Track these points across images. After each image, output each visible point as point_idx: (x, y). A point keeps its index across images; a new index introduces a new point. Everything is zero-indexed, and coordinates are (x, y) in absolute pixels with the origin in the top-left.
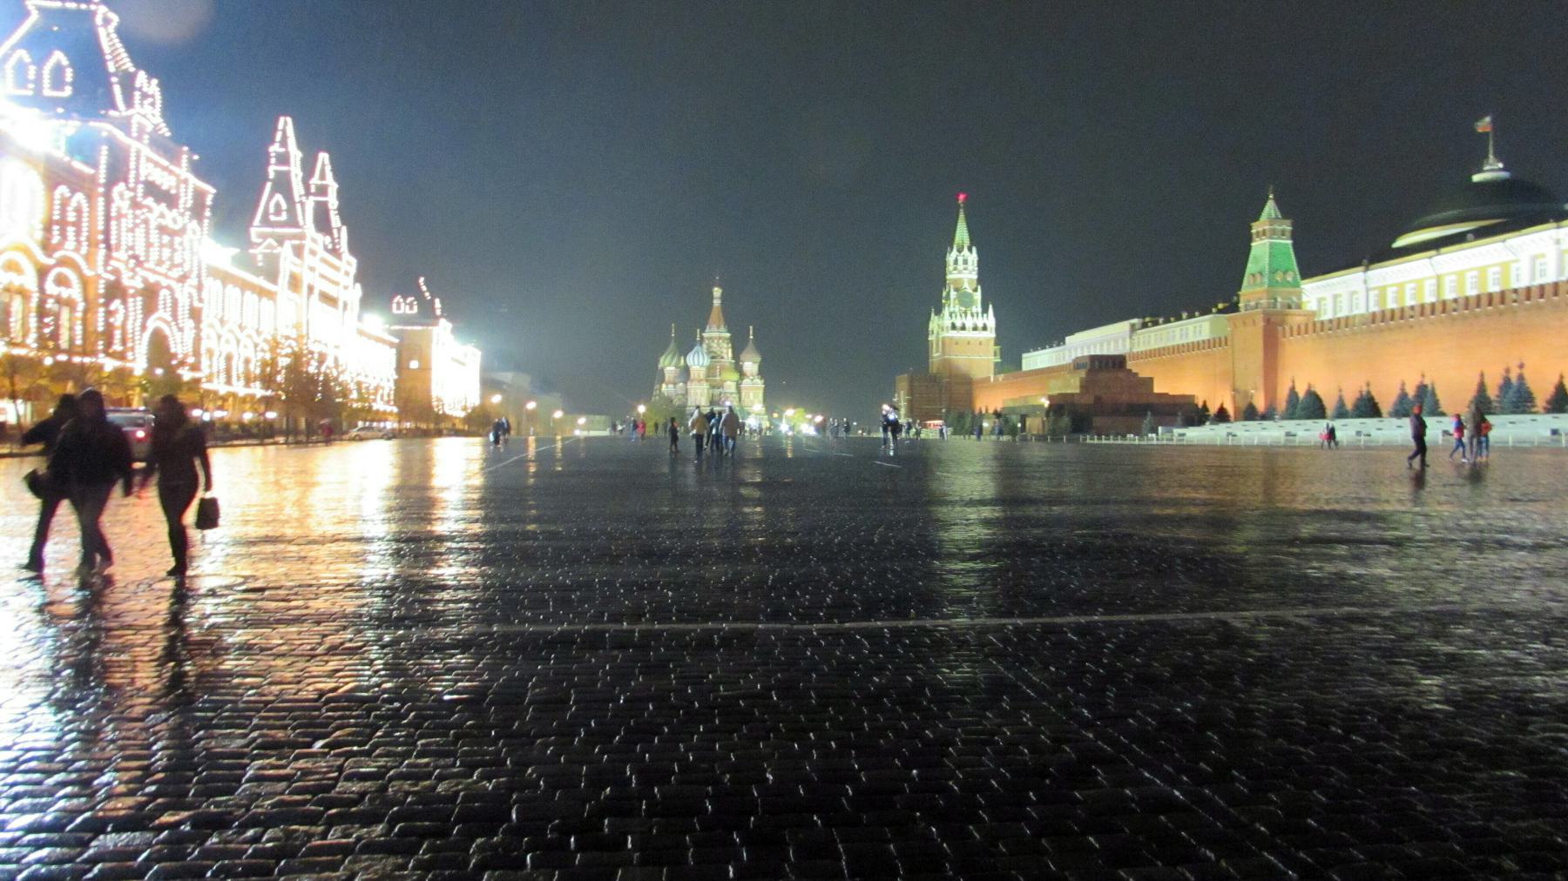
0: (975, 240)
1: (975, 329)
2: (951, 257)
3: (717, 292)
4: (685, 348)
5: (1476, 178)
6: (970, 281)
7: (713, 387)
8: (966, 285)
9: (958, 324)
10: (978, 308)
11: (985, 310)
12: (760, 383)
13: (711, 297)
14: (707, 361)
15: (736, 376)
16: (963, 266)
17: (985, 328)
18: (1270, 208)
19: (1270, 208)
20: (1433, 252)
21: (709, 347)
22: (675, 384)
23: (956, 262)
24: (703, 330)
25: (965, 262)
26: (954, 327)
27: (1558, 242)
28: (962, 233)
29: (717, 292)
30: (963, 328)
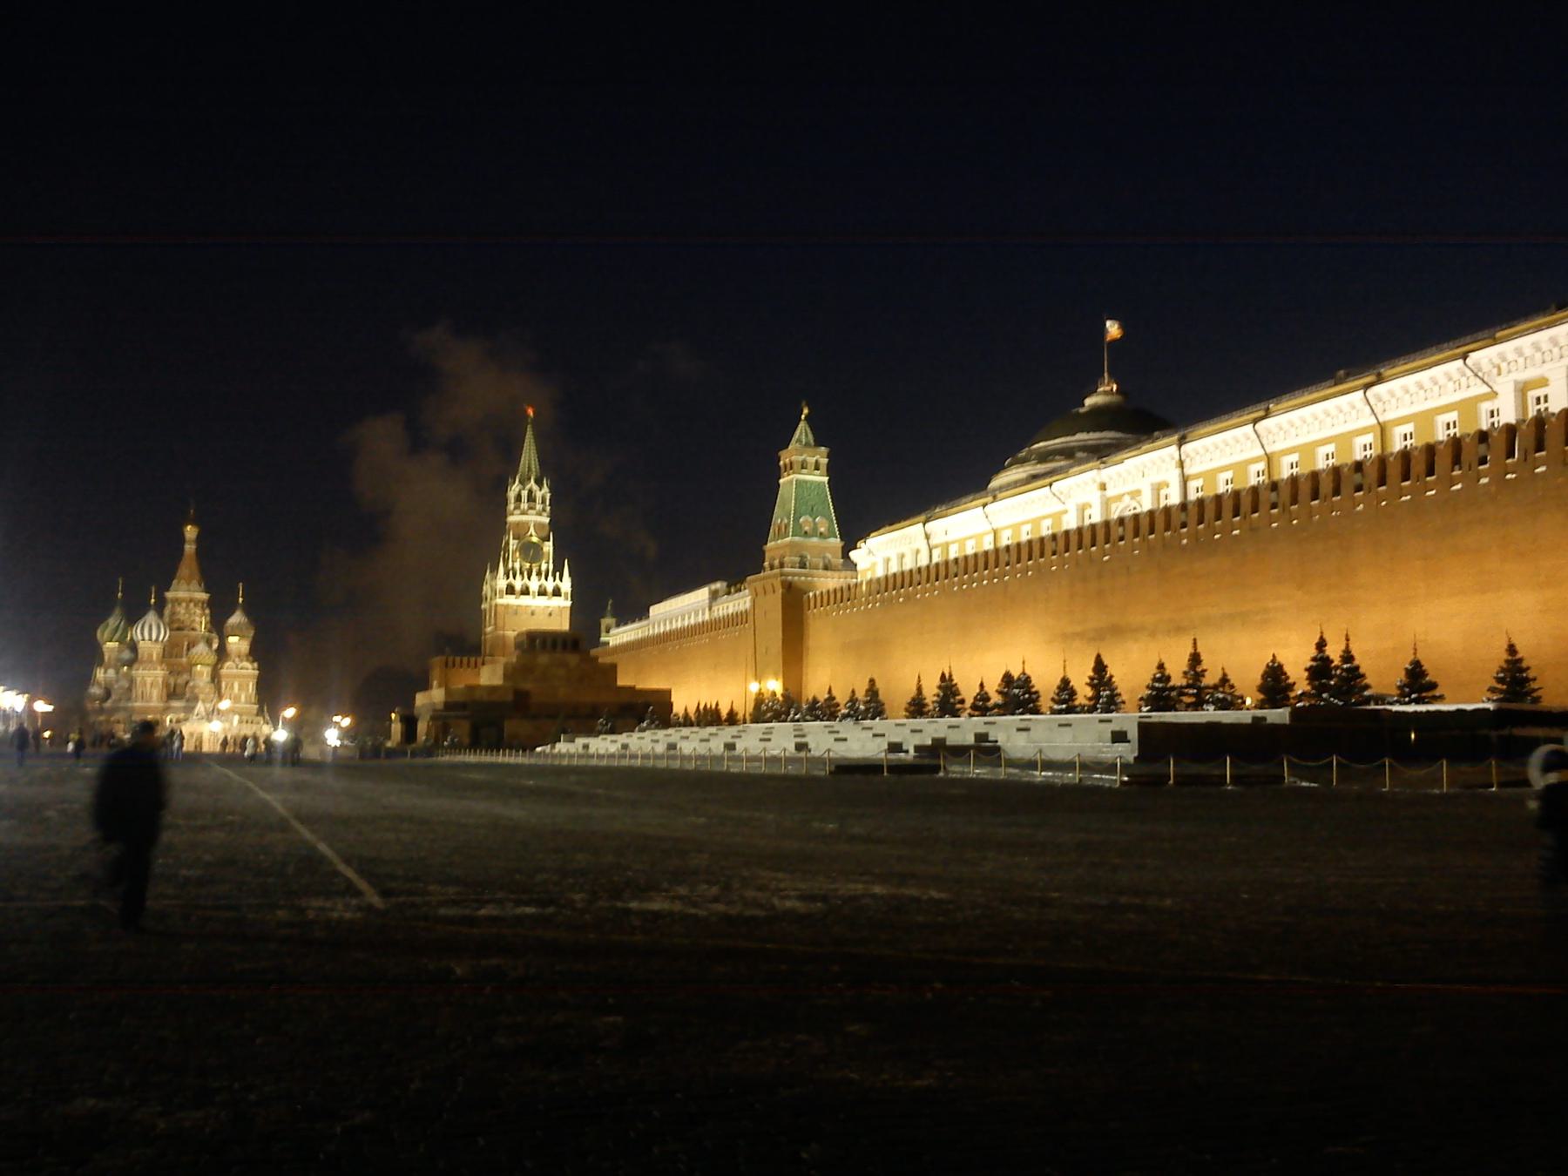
1: (542, 593)
2: (512, 494)
3: (190, 531)
6: (538, 526)
8: (532, 530)
9: (518, 584)
10: (547, 565)
11: (558, 568)
12: (250, 670)
13: (182, 540)
14: (164, 635)
16: (529, 509)
17: (557, 592)
18: (803, 431)
19: (803, 431)
21: (173, 613)
23: (518, 498)
25: (531, 498)
26: (510, 590)
27: (1103, 487)
28: (529, 456)
29: (190, 531)
30: (525, 591)
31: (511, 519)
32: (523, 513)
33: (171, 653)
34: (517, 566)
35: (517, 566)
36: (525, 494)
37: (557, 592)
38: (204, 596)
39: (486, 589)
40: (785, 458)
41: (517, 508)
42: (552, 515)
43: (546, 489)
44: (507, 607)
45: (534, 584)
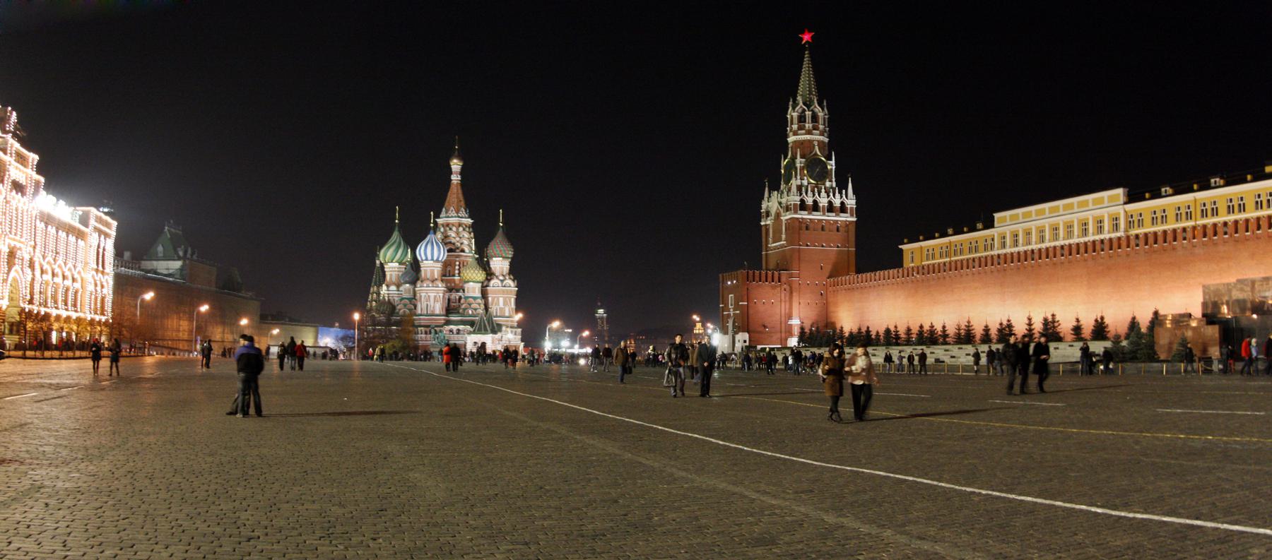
1: (831, 208)
3: (456, 165)
4: (413, 239)
6: (820, 143)
7: (450, 290)
9: (809, 201)
11: (842, 186)
12: (511, 284)
15: (480, 275)
17: (843, 209)
22: (398, 286)
23: (802, 119)
24: (437, 216)
26: (803, 206)
29: (456, 165)
30: (816, 207)
31: (791, 139)
32: (809, 132)
33: (448, 270)
34: (805, 182)
35: (805, 182)
36: (808, 113)
37: (843, 209)
38: (470, 221)
39: (771, 203)
41: (800, 128)
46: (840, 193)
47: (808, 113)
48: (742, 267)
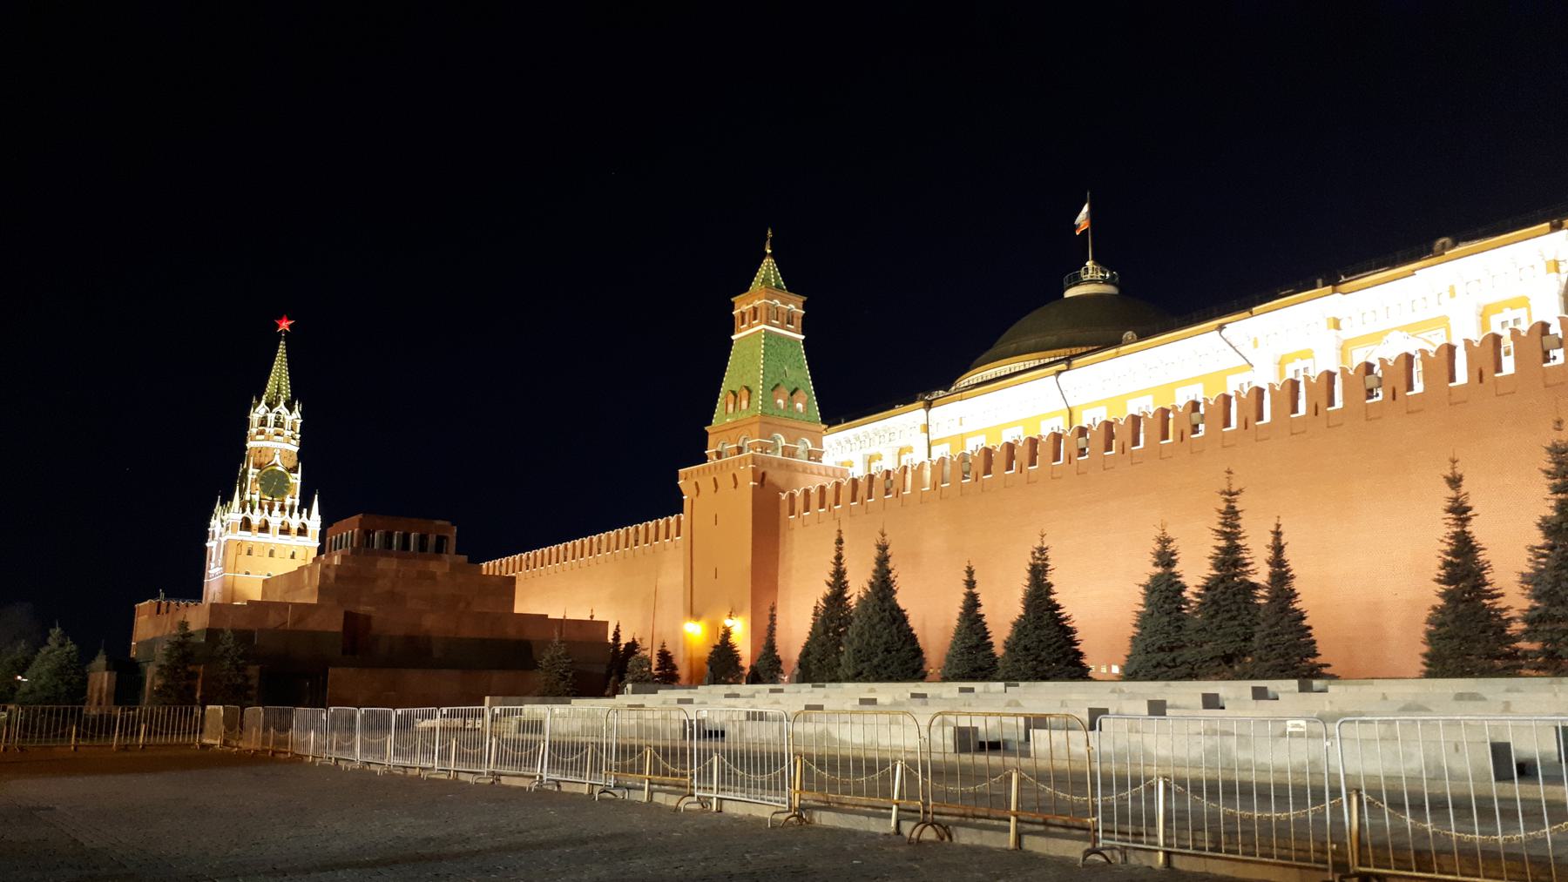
0: (300, 393)
1: (285, 531)
5: (1070, 293)
6: (285, 454)
8: (277, 459)
9: (256, 518)
10: (292, 499)
11: (305, 503)
16: (275, 435)
17: (302, 531)
20: (1063, 366)
23: (263, 422)
25: (279, 424)
26: (246, 525)
28: (279, 377)
30: (264, 528)
31: (250, 444)
34: (256, 498)
36: (271, 417)
37: (302, 531)
39: (215, 524)
40: (742, 306)
42: (301, 445)
43: (296, 414)
44: (240, 544)
45: (276, 520)
46: (300, 512)
47: (271, 417)
48: (155, 596)
